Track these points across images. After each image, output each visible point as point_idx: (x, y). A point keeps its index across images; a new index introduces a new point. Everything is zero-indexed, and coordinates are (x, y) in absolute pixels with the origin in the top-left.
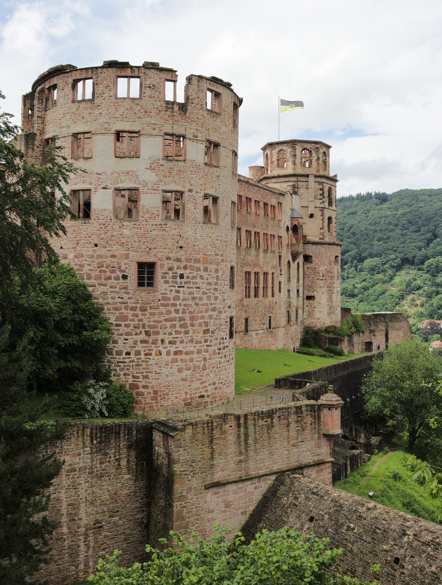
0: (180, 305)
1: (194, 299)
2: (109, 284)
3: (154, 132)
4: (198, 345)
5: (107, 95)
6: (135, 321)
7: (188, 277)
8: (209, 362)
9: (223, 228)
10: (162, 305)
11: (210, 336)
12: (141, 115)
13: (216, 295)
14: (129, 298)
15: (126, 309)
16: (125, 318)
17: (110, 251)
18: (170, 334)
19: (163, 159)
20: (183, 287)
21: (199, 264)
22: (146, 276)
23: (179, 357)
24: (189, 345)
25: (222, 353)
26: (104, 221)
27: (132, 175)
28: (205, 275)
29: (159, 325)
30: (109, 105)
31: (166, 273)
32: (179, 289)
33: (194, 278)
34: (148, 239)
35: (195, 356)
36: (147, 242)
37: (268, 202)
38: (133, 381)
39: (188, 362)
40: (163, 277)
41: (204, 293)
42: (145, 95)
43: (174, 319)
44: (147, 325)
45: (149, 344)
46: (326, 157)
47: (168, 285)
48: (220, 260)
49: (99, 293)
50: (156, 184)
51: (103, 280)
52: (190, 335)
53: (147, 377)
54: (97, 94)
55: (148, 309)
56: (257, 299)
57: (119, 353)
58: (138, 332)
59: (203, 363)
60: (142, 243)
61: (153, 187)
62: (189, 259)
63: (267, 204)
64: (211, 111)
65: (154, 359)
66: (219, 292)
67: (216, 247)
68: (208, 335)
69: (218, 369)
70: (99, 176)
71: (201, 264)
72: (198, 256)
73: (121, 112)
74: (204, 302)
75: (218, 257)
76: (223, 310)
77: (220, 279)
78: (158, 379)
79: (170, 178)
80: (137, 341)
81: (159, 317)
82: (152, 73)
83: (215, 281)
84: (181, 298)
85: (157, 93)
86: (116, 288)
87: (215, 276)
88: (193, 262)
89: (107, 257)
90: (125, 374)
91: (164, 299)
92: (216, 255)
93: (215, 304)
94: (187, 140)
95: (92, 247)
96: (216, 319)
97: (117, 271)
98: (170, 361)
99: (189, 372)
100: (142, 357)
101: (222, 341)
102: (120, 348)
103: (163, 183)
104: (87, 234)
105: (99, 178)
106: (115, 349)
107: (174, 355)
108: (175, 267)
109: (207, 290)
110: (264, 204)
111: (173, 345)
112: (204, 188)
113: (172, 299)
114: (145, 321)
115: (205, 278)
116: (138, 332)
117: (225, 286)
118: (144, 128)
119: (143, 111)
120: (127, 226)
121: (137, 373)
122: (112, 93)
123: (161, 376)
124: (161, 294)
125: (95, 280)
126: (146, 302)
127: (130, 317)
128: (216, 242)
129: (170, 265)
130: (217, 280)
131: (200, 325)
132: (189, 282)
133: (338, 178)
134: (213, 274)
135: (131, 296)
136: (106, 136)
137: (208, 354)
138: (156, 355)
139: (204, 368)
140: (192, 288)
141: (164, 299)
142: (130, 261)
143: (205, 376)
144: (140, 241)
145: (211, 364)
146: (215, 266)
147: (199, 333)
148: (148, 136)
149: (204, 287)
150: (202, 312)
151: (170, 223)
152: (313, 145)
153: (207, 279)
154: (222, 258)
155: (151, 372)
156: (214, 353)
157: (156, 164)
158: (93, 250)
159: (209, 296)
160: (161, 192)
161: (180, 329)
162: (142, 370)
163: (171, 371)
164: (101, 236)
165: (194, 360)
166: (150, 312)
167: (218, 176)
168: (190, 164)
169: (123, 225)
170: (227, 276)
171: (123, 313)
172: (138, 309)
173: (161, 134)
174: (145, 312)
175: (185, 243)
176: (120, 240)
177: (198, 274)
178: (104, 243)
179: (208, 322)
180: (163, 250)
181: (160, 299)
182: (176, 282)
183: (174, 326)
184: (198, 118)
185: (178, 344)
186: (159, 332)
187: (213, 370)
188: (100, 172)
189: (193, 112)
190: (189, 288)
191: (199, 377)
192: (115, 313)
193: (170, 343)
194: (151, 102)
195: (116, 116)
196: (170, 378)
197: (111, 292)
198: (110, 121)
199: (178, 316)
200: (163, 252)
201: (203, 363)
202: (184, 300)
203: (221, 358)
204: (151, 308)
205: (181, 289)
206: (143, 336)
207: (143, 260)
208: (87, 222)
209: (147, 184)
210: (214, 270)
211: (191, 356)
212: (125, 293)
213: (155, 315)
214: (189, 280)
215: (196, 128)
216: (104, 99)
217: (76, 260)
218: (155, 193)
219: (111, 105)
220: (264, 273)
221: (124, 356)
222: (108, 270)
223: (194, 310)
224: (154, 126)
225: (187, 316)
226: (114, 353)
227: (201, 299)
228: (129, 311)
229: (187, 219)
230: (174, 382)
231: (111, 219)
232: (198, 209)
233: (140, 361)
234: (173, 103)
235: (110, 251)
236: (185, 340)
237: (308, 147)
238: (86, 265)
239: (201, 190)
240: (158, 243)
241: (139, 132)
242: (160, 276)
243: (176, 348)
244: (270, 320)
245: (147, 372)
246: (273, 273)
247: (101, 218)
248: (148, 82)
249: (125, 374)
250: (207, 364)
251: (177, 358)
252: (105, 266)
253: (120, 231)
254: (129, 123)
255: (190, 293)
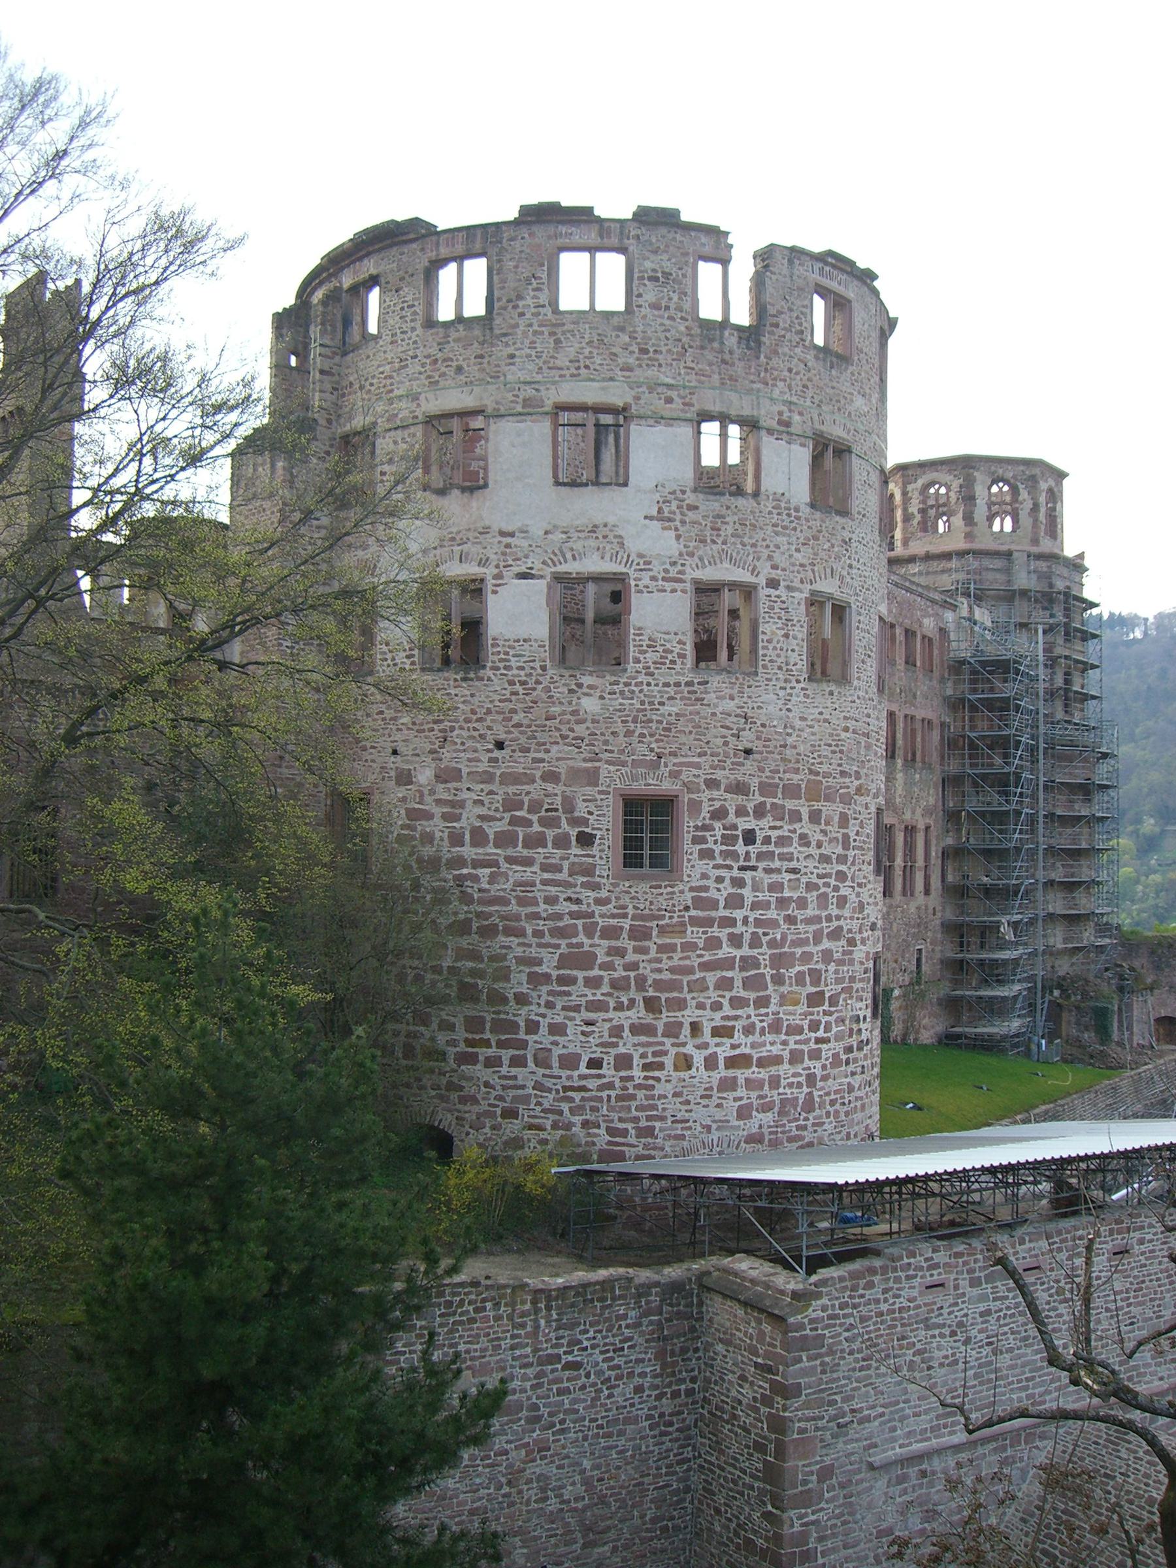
0: (745, 921)
1: (782, 903)
2: (539, 859)
3: (668, 410)
4: (792, 1039)
5: (529, 301)
6: (615, 970)
7: (767, 840)
8: (822, 1089)
9: (861, 693)
10: (694, 921)
11: (825, 1013)
12: (631, 360)
13: (843, 892)
14: (599, 902)
15: (589, 931)
16: (585, 960)
17: (542, 761)
18: (717, 1006)
19: (695, 490)
20: (754, 868)
21: (796, 802)
22: (646, 836)
23: (741, 1075)
24: (769, 1038)
25: (856, 1060)
26: (522, 673)
27: (605, 537)
28: (814, 833)
29: (685, 979)
30: (535, 333)
31: (705, 828)
32: (742, 874)
33: (782, 841)
34: (654, 725)
35: (785, 1069)
36: (651, 735)
37: (915, 627)
38: (609, 1143)
39: (766, 1087)
40: (696, 840)
41: (810, 887)
42: (640, 301)
43: (728, 963)
44: (650, 982)
45: (656, 1035)
46: (1055, 503)
47: (712, 863)
48: (852, 791)
49: (509, 886)
50: (674, 564)
51: (519, 848)
52: (773, 1008)
53: (649, 1132)
54: (499, 299)
55: (654, 933)
56: (888, 900)
57: (569, 1062)
58: (625, 1000)
59: (805, 1090)
60: (635, 739)
61: (666, 571)
62: (770, 785)
63: (914, 633)
64: (825, 350)
65: (669, 1080)
66: (847, 884)
67: (841, 752)
68: (821, 1009)
69: (846, 1108)
70: (509, 540)
71: (802, 801)
72: (796, 778)
73: (572, 352)
74: (810, 912)
75: (847, 780)
76: (858, 937)
77: (853, 844)
78: (683, 1137)
79: (714, 547)
80: (621, 1028)
81: (688, 958)
82: (656, 236)
83: (839, 850)
84: (748, 902)
85: (675, 297)
86: (560, 871)
87: (840, 836)
88: (780, 795)
89: (534, 781)
90: (586, 1124)
91: (699, 903)
92: (843, 774)
93: (838, 918)
94: (763, 433)
95: (489, 751)
96: (840, 962)
97: (564, 821)
98: (715, 1084)
99: (768, 1118)
100: (637, 1073)
101: (855, 1027)
102: (572, 1049)
103: (696, 559)
104: (473, 712)
105: (508, 546)
106: (557, 1052)
107: (727, 1068)
108: (732, 811)
109: (819, 876)
110: (907, 631)
111: (725, 1040)
112: (810, 574)
113: (722, 904)
114: (645, 969)
115: (814, 844)
116: (625, 1000)
117: (864, 867)
118: (638, 398)
119: (635, 348)
120: (590, 687)
121: (621, 1120)
122: (544, 298)
123: (690, 1128)
124: (692, 889)
125: (496, 846)
126: (647, 912)
127: (602, 958)
128: (843, 735)
129: (717, 804)
130: (843, 849)
131: (800, 979)
132: (770, 855)
133: (1087, 563)
134: (834, 830)
135: (604, 894)
136: (526, 425)
137: (818, 1065)
138: (676, 1069)
139: (809, 1105)
140: (778, 871)
141: (699, 903)
142: (600, 792)
143: (810, 1129)
144: (629, 733)
145: (828, 1094)
146: (840, 808)
147: (796, 1003)
148: (651, 422)
149: (811, 869)
150: (803, 942)
151: (718, 678)
152: (1022, 468)
153: (819, 845)
154: (857, 783)
155: (662, 1119)
156: (836, 1061)
157: (674, 504)
158: (491, 760)
159: (825, 896)
160: (688, 586)
161: (743, 994)
162: (634, 1113)
163: (719, 1115)
164: (516, 718)
165: (783, 1082)
166: (659, 942)
167: (846, 543)
168: (770, 505)
169: (580, 686)
170: (868, 836)
171: (581, 945)
172: (625, 935)
173: (688, 415)
174: (646, 943)
175: (758, 738)
176: (572, 730)
177: (794, 831)
178: (523, 740)
179: (820, 971)
180: (696, 760)
181: (689, 903)
182: (734, 855)
183: (725, 984)
184: (790, 370)
185: (739, 1037)
186: (685, 1000)
187: (831, 1110)
188: (510, 529)
189: (776, 353)
190: (768, 871)
191: (795, 1132)
192: (558, 946)
193: (716, 1032)
194: (659, 321)
195: (559, 363)
196: (715, 1135)
197: (545, 882)
198: (539, 378)
199: (738, 953)
200: (698, 766)
201: (805, 1090)
202: (755, 906)
203: (853, 1074)
204: (662, 930)
205: (748, 876)
206: (638, 1014)
207: (639, 787)
208: (472, 675)
209: (649, 563)
210: (836, 819)
211: (773, 1070)
212: (583, 885)
213: (674, 951)
214: (772, 848)
215: (787, 397)
216: (522, 314)
217: (440, 787)
218: (674, 591)
219: (542, 333)
220: (906, 827)
221: (583, 1070)
222: (534, 818)
223: (784, 937)
224: (669, 393)
225: (764, 954)
226: (555, 1064)
227: (802, 903)
228: (597, 941)
229: (764, 667)
230: (725, 1145)
231: (544, 668)
232: (795, 638)
233: (629, 1085)
234: (725, 323)
235: (542, 761)
236: (759, 1025)
237: (1009, 475)
238: (469, 803)
239: (802, 582)
240: (683, 738)
241: (624, 409)
242: (688, 838)
243: (733, 1047)
244: (919, 960)
245: (649, 1118)
246: (927, 828)
247: (514, 662)
248: (648, 265)
249: (586, 1124)
250: (816, 1094)
251: (735, 1078)
252: (526, 807)
253: (570, 703)
254: (595, 384)
255: (775, 887)
